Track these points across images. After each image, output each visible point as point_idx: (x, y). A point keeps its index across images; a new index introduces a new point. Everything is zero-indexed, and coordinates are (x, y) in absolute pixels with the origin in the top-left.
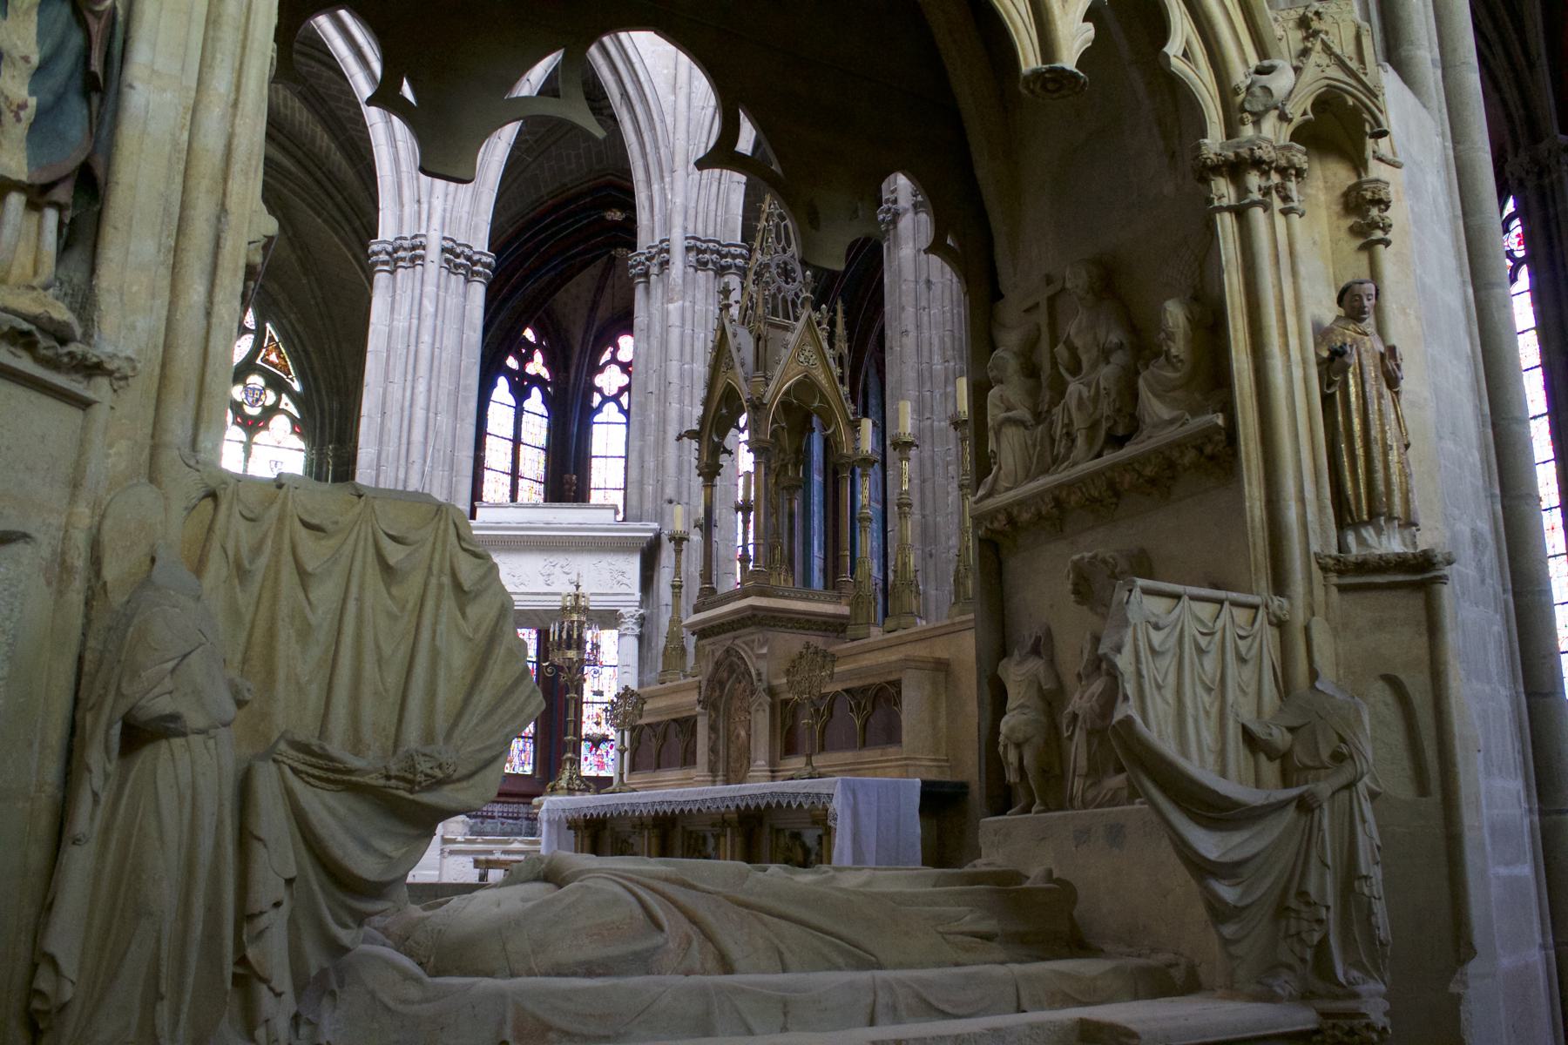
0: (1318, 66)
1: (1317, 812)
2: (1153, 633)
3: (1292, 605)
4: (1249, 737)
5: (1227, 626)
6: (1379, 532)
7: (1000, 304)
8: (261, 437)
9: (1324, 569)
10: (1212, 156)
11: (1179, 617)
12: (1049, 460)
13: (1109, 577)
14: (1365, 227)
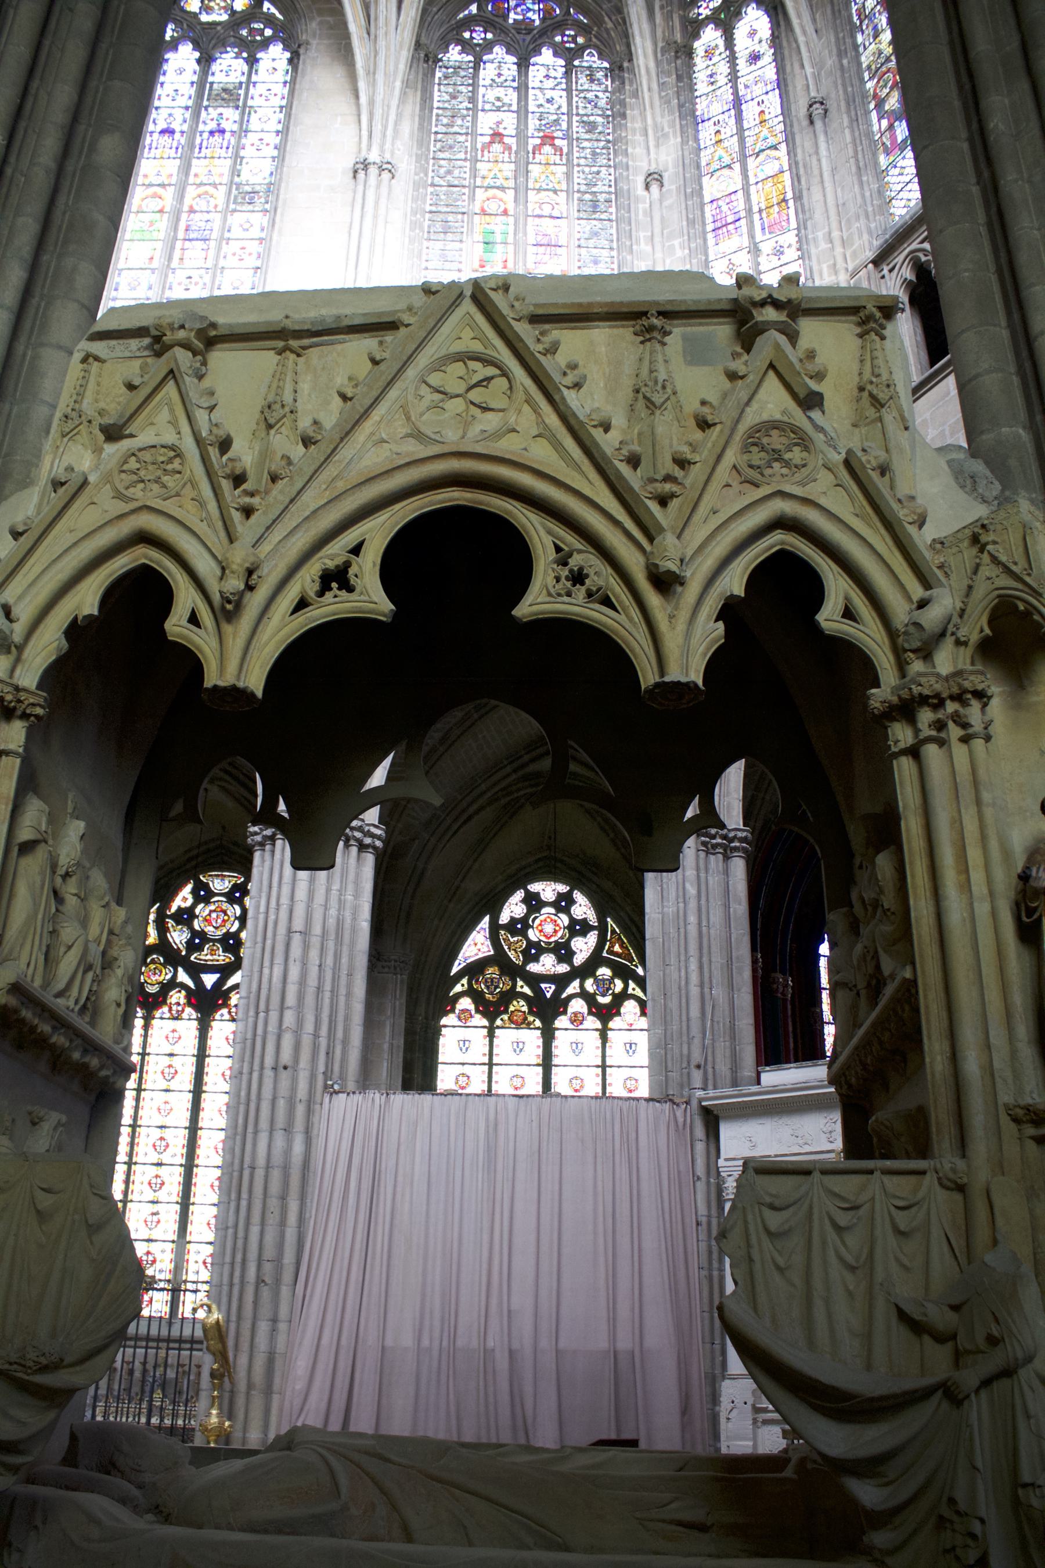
2: (767, 1213)
3: (969, 1166)
4: (902, 1315)
5: (877, 1197)
8: (615, 1023)
9: (1016, 1120)
10: (877, 705)
11: (807, 1193)
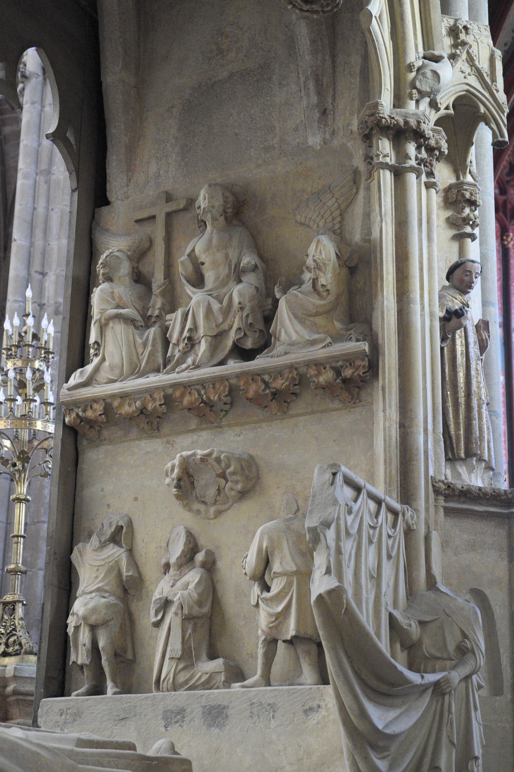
0: (462, 72)
1: (447, 697)
6: (471, 470)
7: (105, 210)
9: (437, 492)
12: (161, 361)
13: (219, 476)
14: (460, 222)
